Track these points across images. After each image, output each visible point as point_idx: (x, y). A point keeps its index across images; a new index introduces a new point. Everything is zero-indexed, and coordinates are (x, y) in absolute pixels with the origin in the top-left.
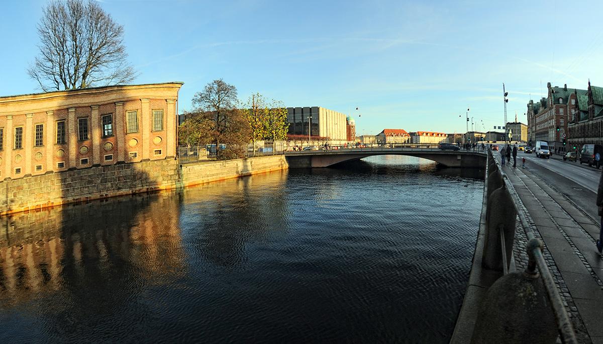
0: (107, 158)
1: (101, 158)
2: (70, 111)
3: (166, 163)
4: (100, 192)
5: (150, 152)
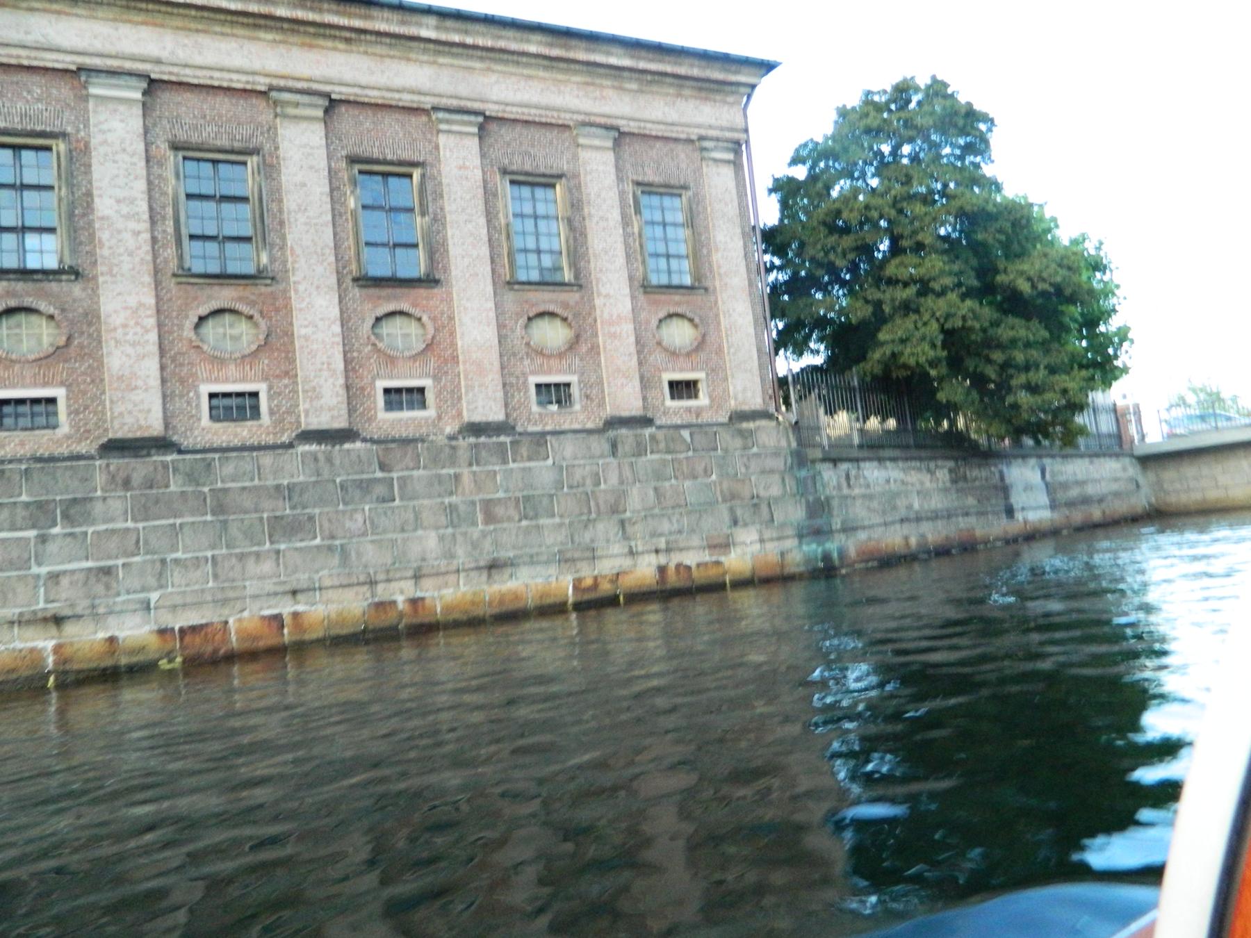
0: (394, 396)
1: (353, 393)
2: (93, 90)
4: (372, 583)
5: (646, 383)
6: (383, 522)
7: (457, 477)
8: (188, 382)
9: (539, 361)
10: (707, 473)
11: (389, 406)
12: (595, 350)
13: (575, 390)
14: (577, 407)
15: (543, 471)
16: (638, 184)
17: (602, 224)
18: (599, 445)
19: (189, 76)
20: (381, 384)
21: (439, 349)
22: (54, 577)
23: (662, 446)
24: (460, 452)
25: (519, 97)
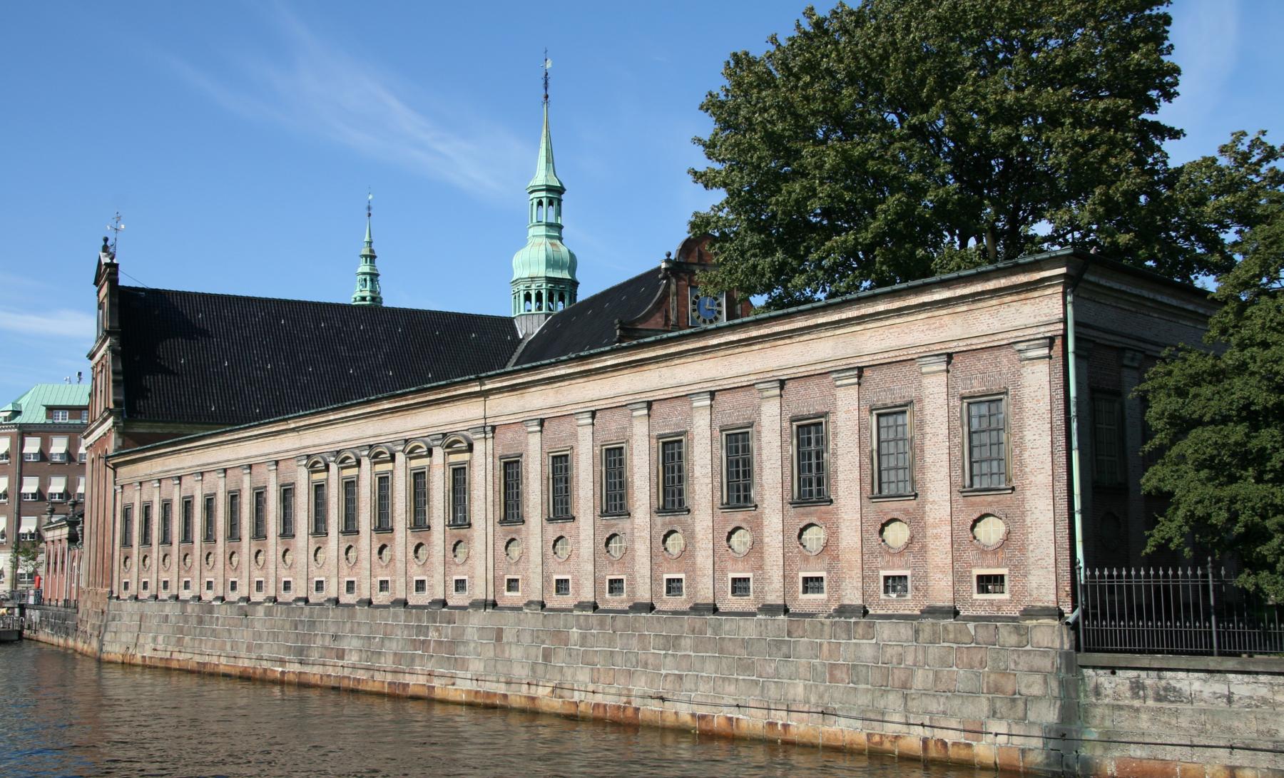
2: (695, 404)
3: (1013, 639)
5: (959, 578)
6: (783, 671)
7: (821, 645)
8: (724, 571)
9: (887, 558)
10: (982, 664)
11: (805, 591)
12: (924, 548)
14: (909, 596)
15: (867, 649)
16: (963, 398)
17: (934, 440)
18: (905, 630)
20: (802, 574)
22: (666, 676)
23: (951, 636)
24: (826, 628)
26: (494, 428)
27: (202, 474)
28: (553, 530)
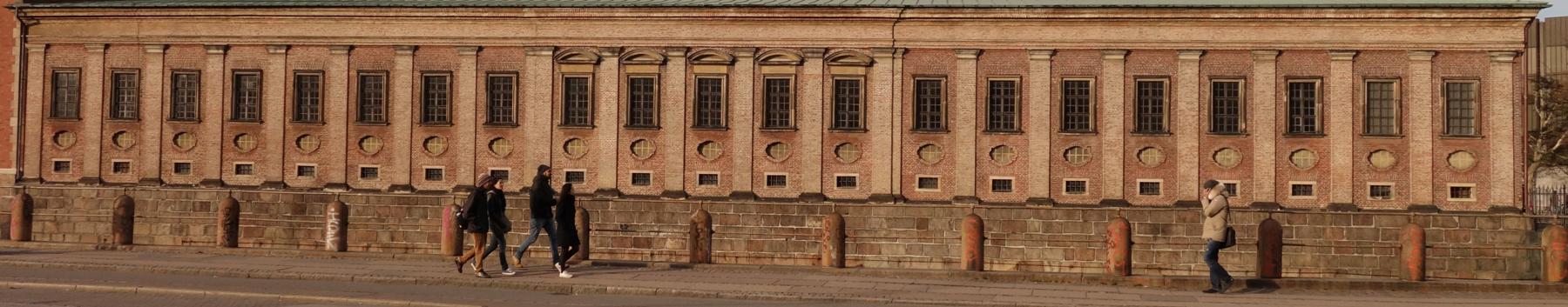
0: (1297, 190)
11: (1294, 194)
12: (1406, 170)
13: (1393, 190)
19: (1218, 47)
21: (1321, 167)
25: (1378, 38)
26: (906, 51)
27: (289, 47)
28: (988, 142)
